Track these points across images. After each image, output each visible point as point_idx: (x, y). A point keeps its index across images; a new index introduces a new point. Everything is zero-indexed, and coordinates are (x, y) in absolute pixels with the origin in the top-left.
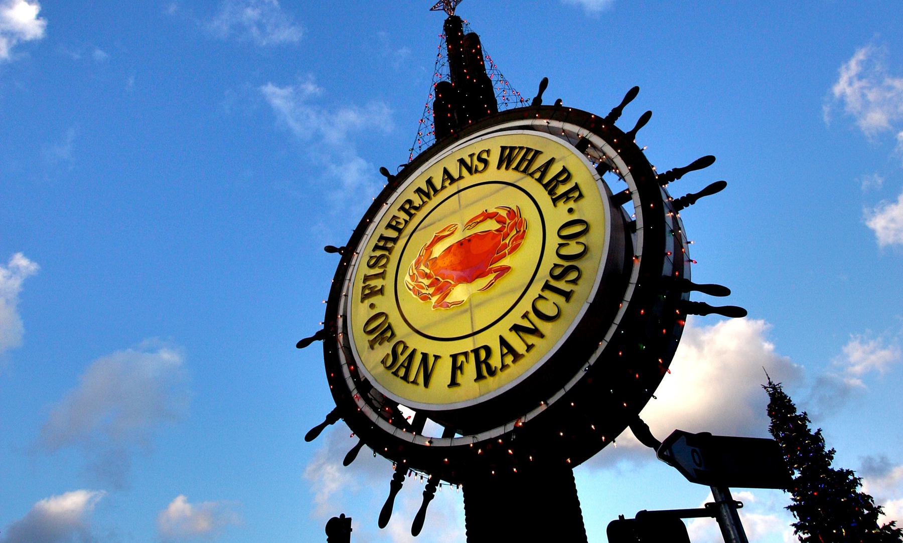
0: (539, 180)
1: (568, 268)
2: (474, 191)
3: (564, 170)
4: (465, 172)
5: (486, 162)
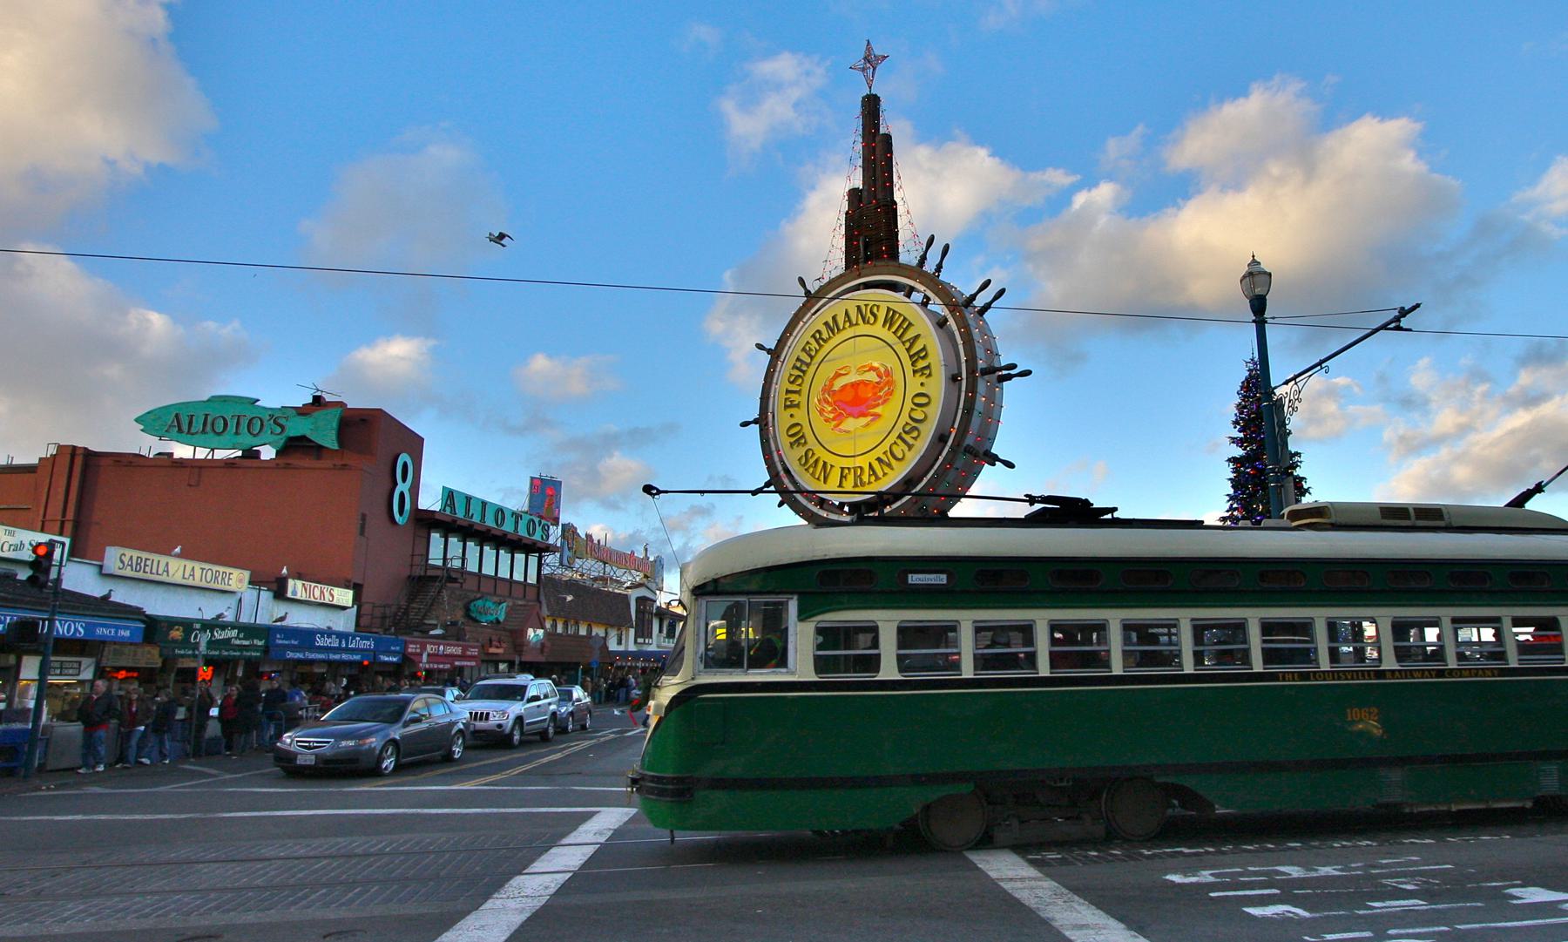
0: (908, 350)
1: (913, 427)
2: (862, 352)
5: (875, 316)
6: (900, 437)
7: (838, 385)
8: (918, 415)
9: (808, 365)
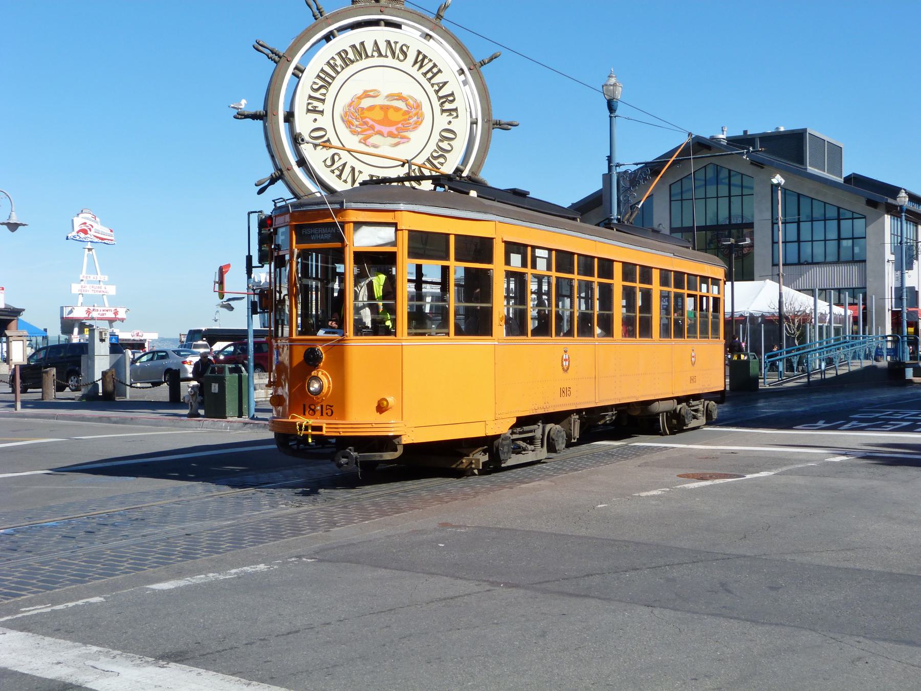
0: (437, 92)
3: (452, 94)
4: (389, 54)
6: (428, 160)
7: (366, 103)
8: (445, 145)
9: (333, 78)
